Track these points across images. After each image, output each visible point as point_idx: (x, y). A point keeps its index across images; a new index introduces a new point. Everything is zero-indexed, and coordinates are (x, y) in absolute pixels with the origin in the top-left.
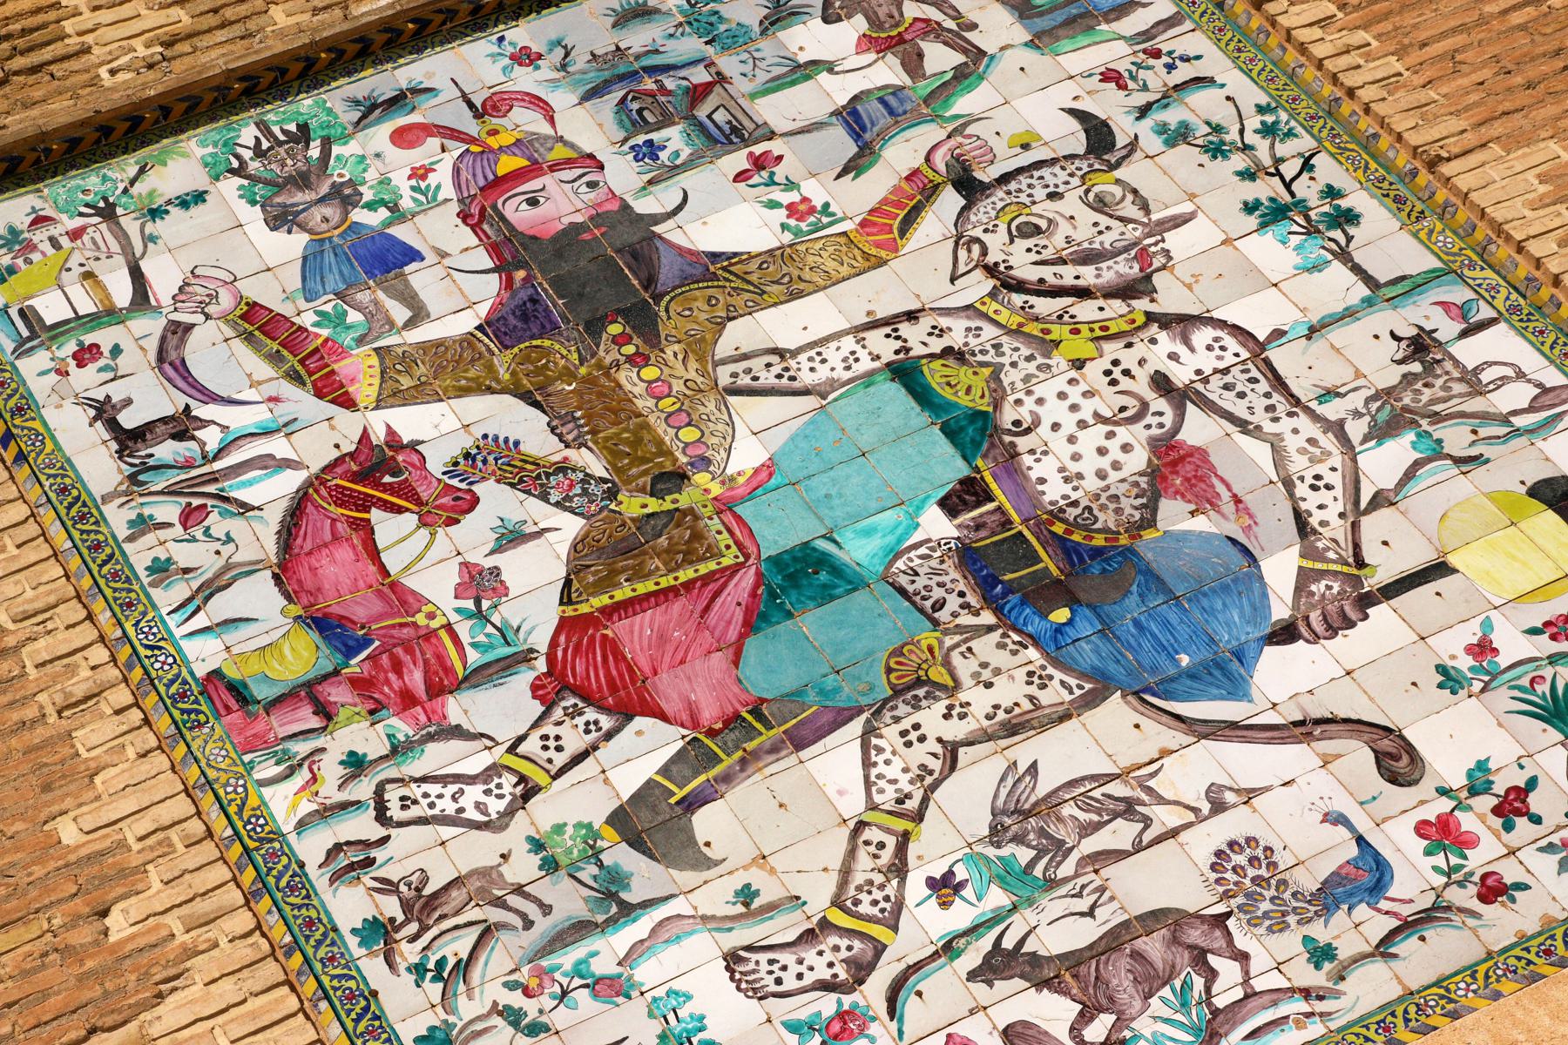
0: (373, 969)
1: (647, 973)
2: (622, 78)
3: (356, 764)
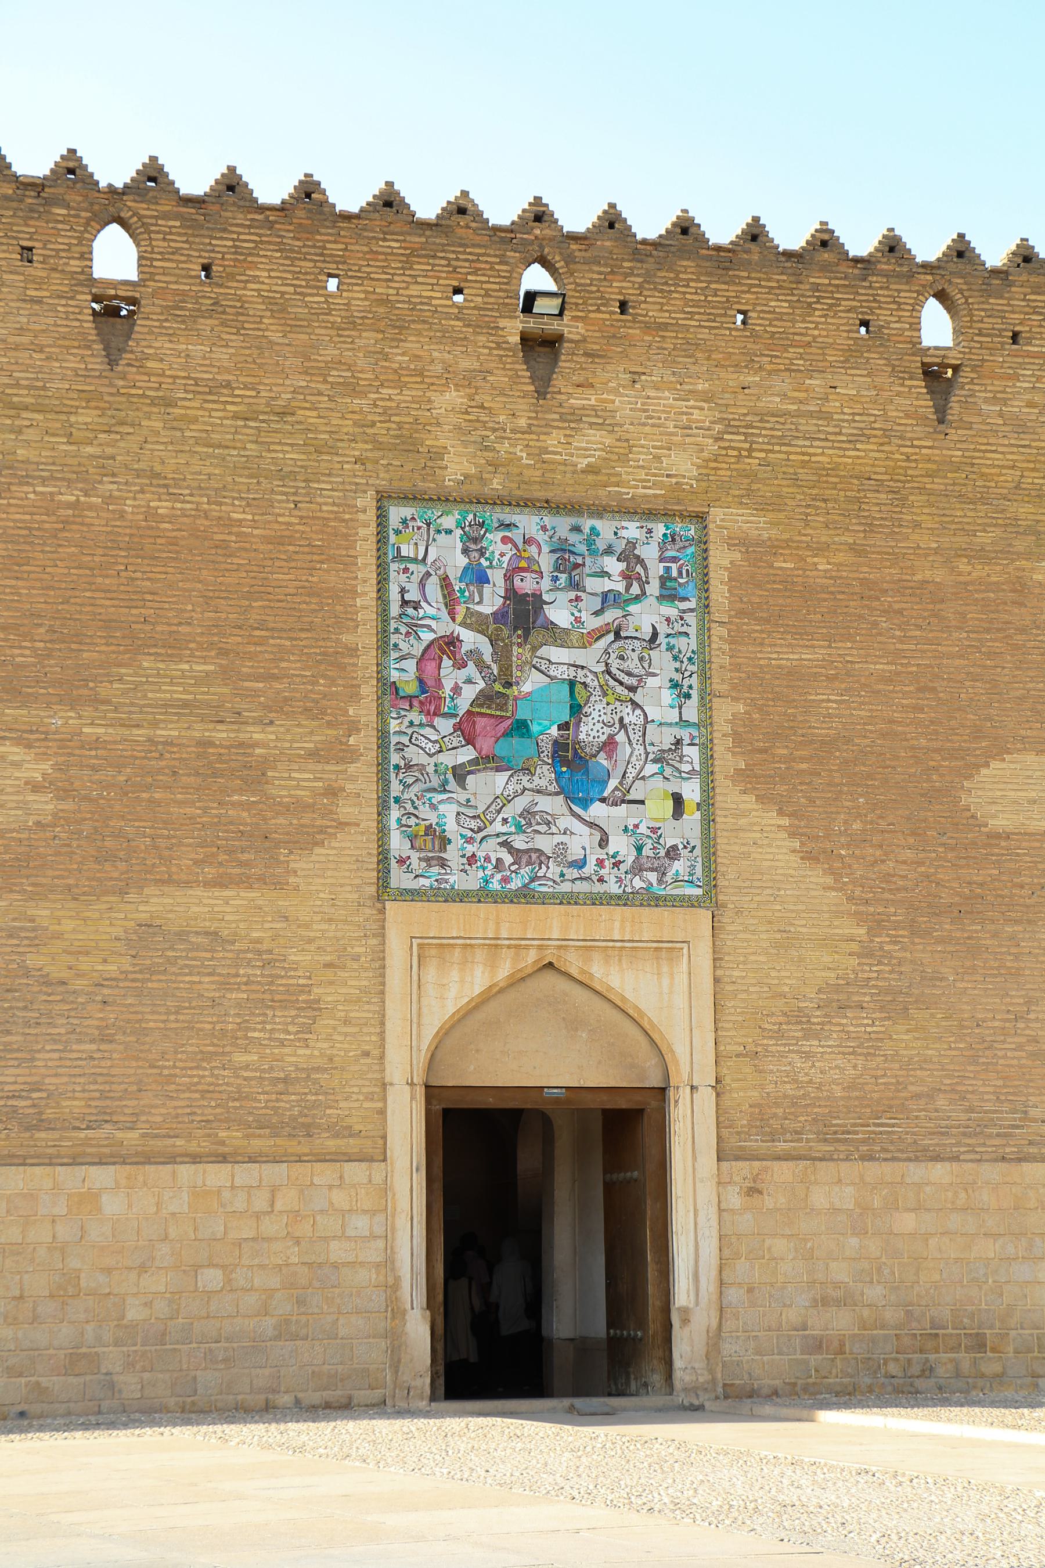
0: (393, 776)
1: (441, 807)
2: (562, 550)
3: (411, 724)
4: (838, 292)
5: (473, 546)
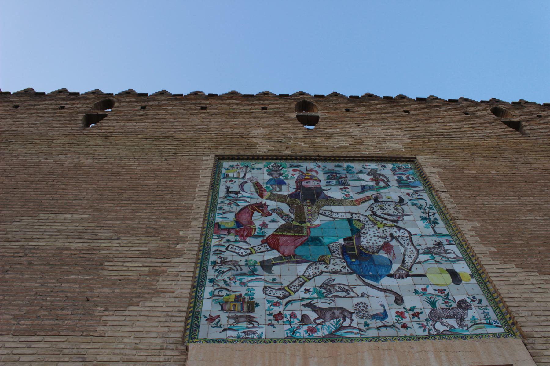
1: (250, 284)
3: (228, 241)
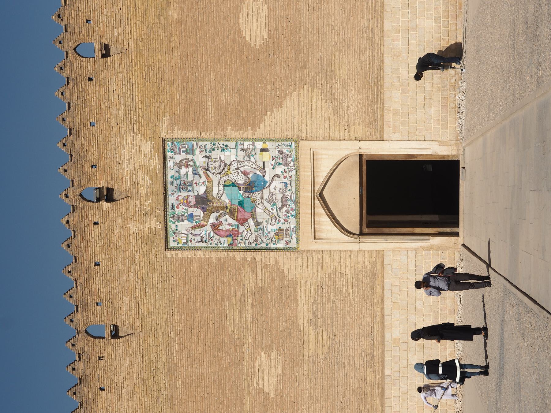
0: (259, 246)
1: (269, 230)
3: (241, 240)
4: (80, 89)
5: (181, 218)
